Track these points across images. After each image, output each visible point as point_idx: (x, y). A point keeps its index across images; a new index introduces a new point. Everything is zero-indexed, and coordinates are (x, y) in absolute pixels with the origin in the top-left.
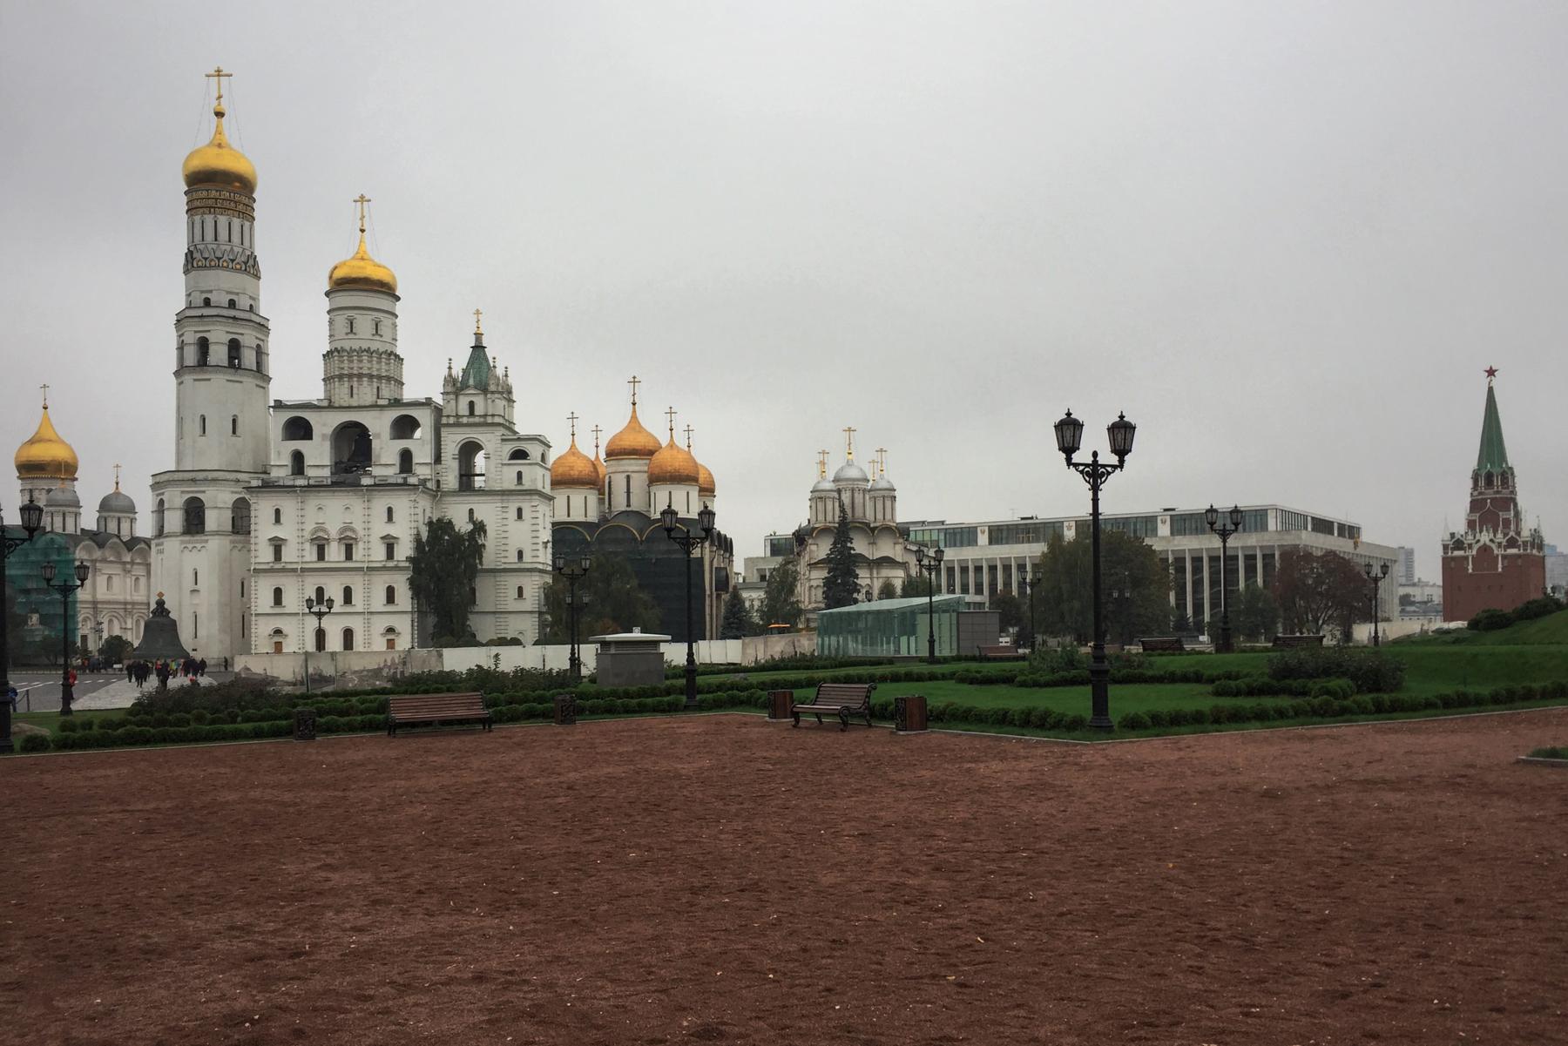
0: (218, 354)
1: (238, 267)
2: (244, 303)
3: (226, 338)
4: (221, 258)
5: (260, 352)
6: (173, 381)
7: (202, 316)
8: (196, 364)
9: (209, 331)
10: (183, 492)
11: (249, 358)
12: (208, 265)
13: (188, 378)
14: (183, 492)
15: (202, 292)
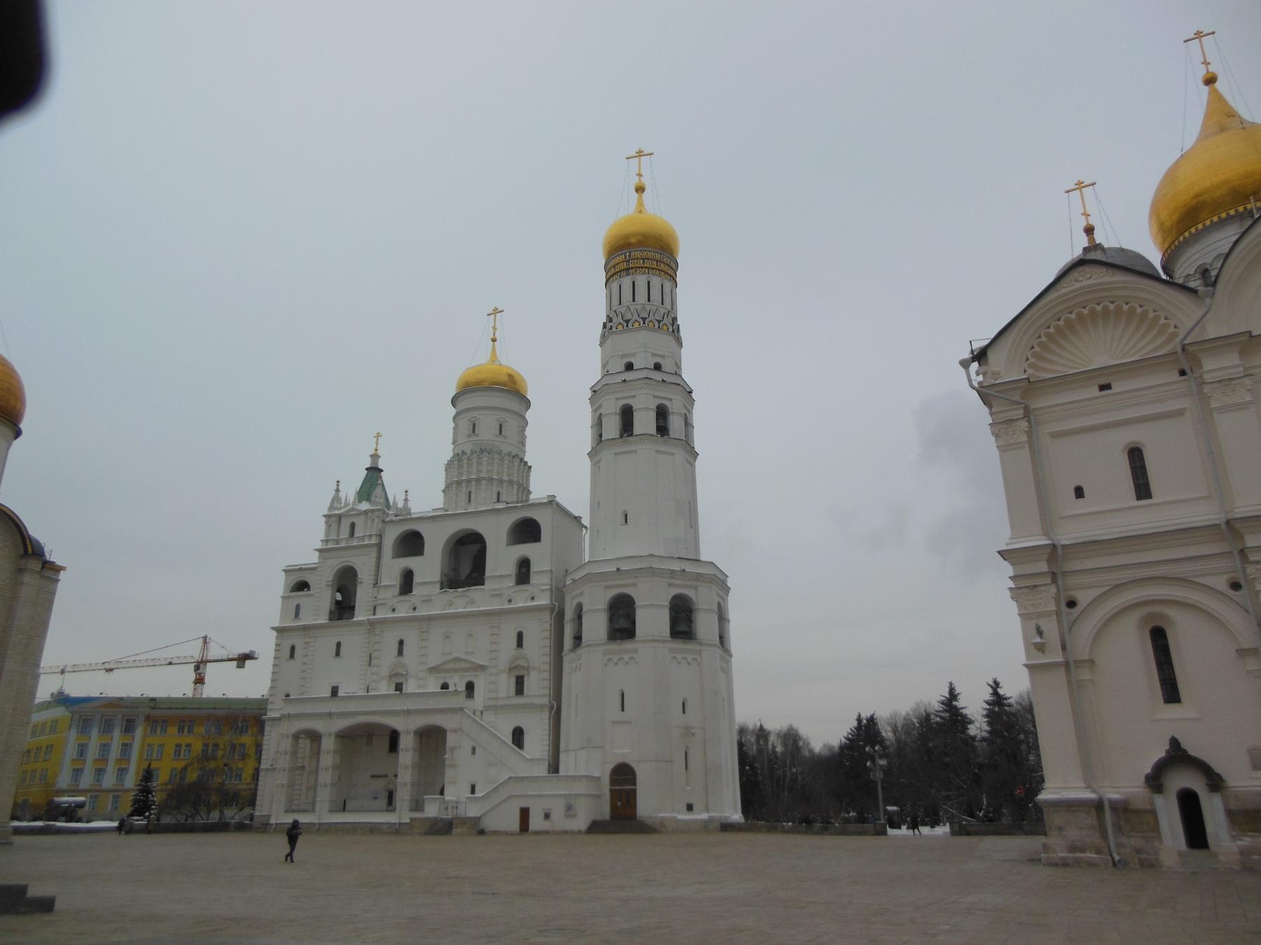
0: (645, 422)
1: (665, 328)
2: (667, 365)
3: (653, 404)
4: (646, 318)
5: (688, 424)
6: (587, 463)
7: (625, 380)
8: (618, 436)
9: (634, 396)
10: (606, 587)
11: (675, 423)
12: (630, 326)
13: (606, 455)
14: (606, 587)
15: (623, 356)
